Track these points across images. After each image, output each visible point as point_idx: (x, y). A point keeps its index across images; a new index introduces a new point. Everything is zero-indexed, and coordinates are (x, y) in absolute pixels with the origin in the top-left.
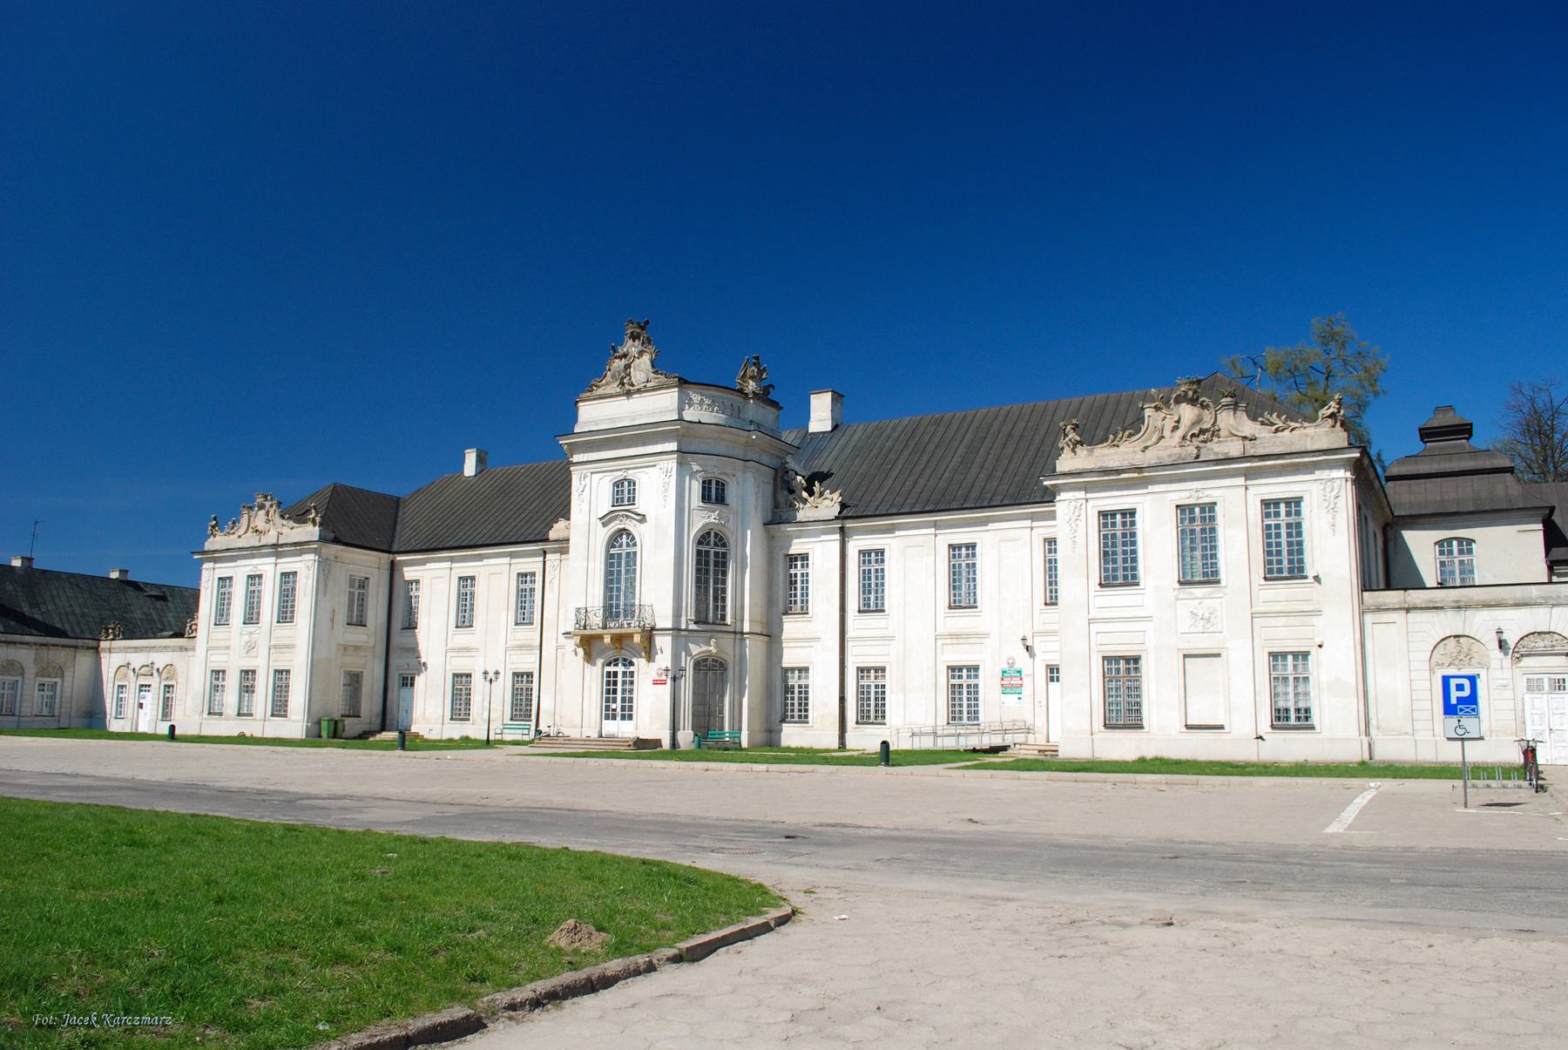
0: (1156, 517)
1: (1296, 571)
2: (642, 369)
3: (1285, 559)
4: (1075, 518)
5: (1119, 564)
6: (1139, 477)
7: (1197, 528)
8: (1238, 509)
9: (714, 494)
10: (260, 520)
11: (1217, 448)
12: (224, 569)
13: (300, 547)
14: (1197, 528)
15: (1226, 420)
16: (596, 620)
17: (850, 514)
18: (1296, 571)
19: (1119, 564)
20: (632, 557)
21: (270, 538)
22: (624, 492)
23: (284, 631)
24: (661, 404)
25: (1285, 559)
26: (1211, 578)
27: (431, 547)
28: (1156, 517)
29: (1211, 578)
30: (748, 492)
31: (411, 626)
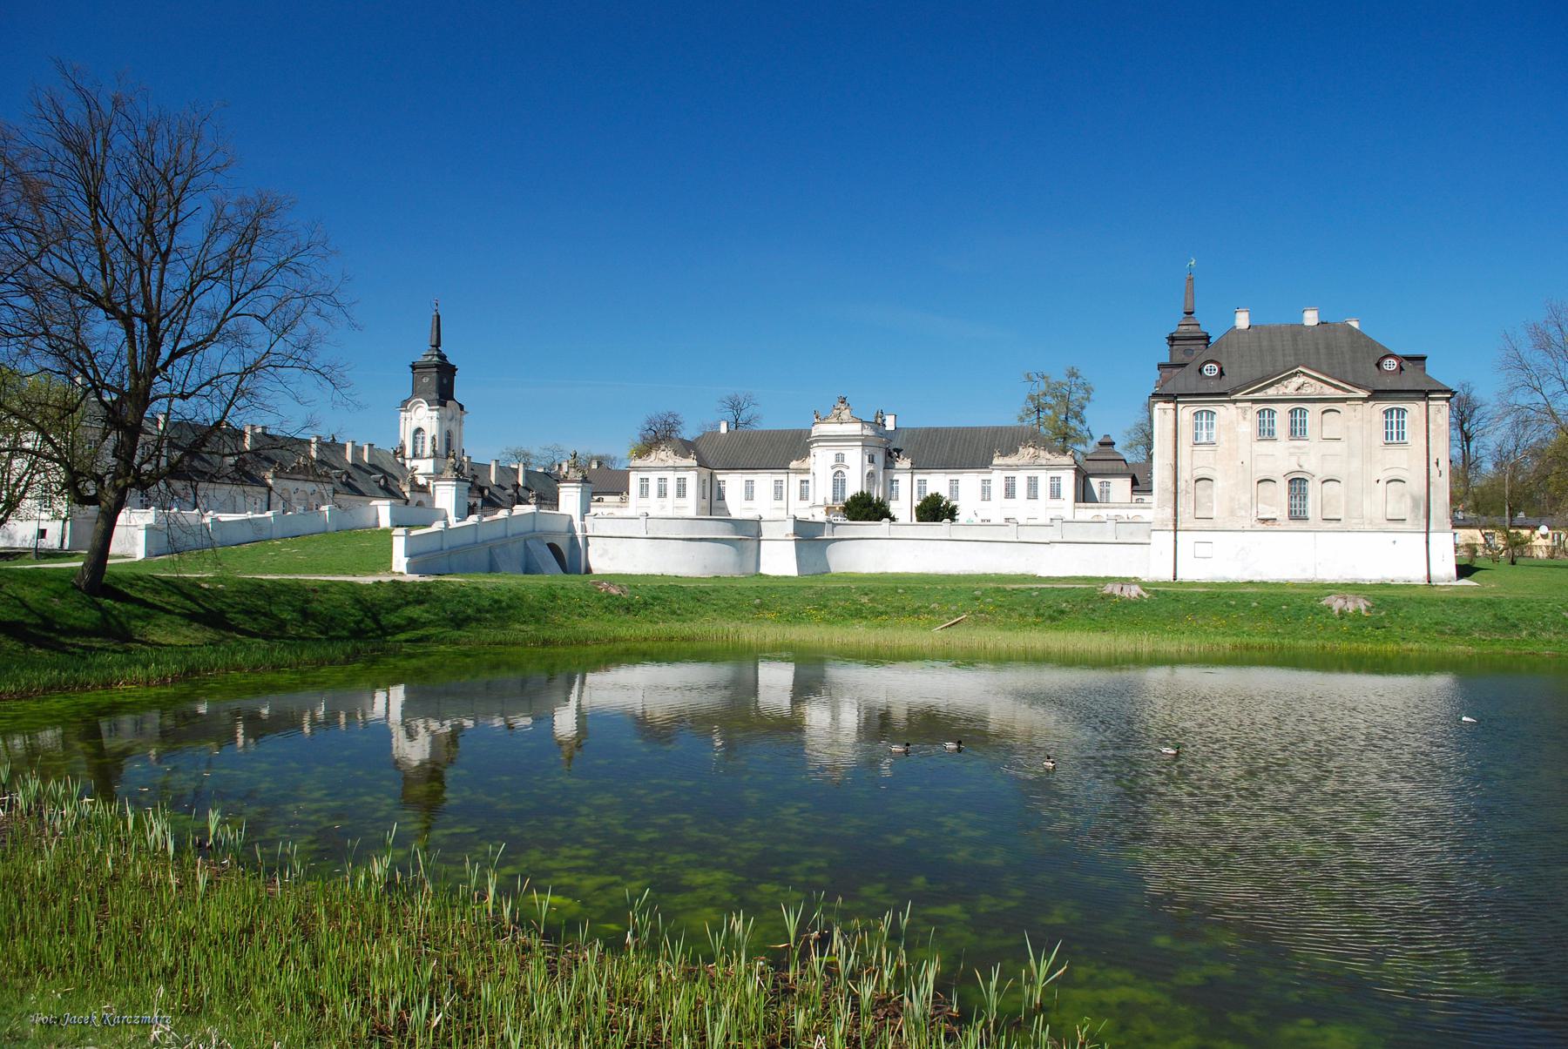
0: (1021, 478)
1: (1058, 497)
2: (846, 415)
3: (1055, 493)
4: (997, 478)
5: (1010, 492)
6: (1017, 468)
7: (1033, 484)
8: (1044, 478)
9: (871, 461)
10: (662, 455)
11: (1040, 461)
12: (644, 475)
13: (688, 468)
14: (1033, 484)
15: (1042, 453)
16: (830, 501)
17: (916, 467)
18: (1058, 497)
19: (1010, 492)
20: (843, 481)
21: (670, 463)
22: (840, 458)
23: (681, 501)
24: (855, 429)
25: (1055, 493)
26: (1036, 497)
27: (731, 467)
28: (1021, 478)
29: (1036, 497)
30: (880, 458)
31: (722, 498)
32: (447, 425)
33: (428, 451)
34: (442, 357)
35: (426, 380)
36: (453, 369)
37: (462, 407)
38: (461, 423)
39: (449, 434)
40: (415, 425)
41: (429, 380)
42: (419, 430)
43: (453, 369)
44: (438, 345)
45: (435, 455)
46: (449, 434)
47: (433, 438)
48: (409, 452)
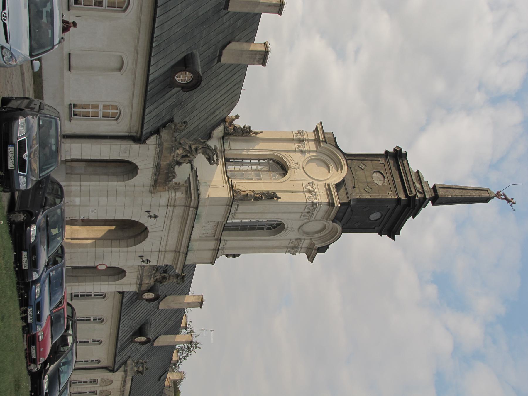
32: (292, 222)
33: (245, 185)
34: (410, 206)
35: (377, 178)
36: (392, 229)
37: (322, 250)
38: (293, 249)
39: (277, 227)
40: (294, 159)
41: (380, 186)
42: (281, 167)
43: (392, 229)
44: (437, 200)
45: (237, 198)
46: (277, 227)
47: (271, 196)
48: (236, 147)
